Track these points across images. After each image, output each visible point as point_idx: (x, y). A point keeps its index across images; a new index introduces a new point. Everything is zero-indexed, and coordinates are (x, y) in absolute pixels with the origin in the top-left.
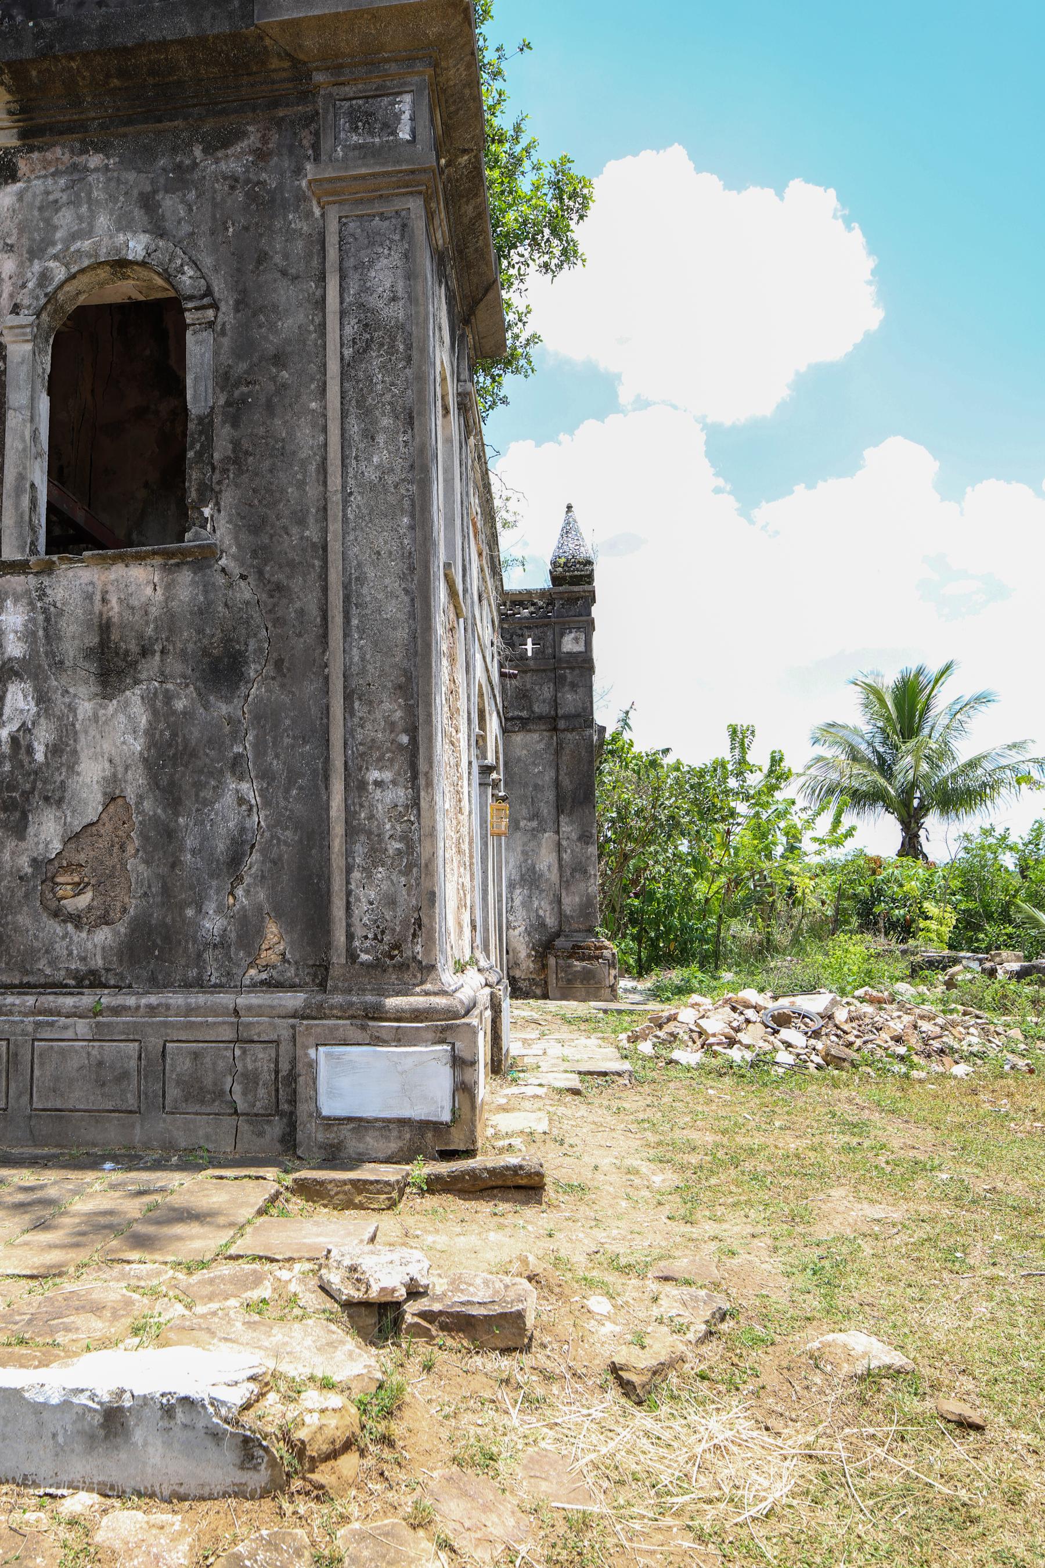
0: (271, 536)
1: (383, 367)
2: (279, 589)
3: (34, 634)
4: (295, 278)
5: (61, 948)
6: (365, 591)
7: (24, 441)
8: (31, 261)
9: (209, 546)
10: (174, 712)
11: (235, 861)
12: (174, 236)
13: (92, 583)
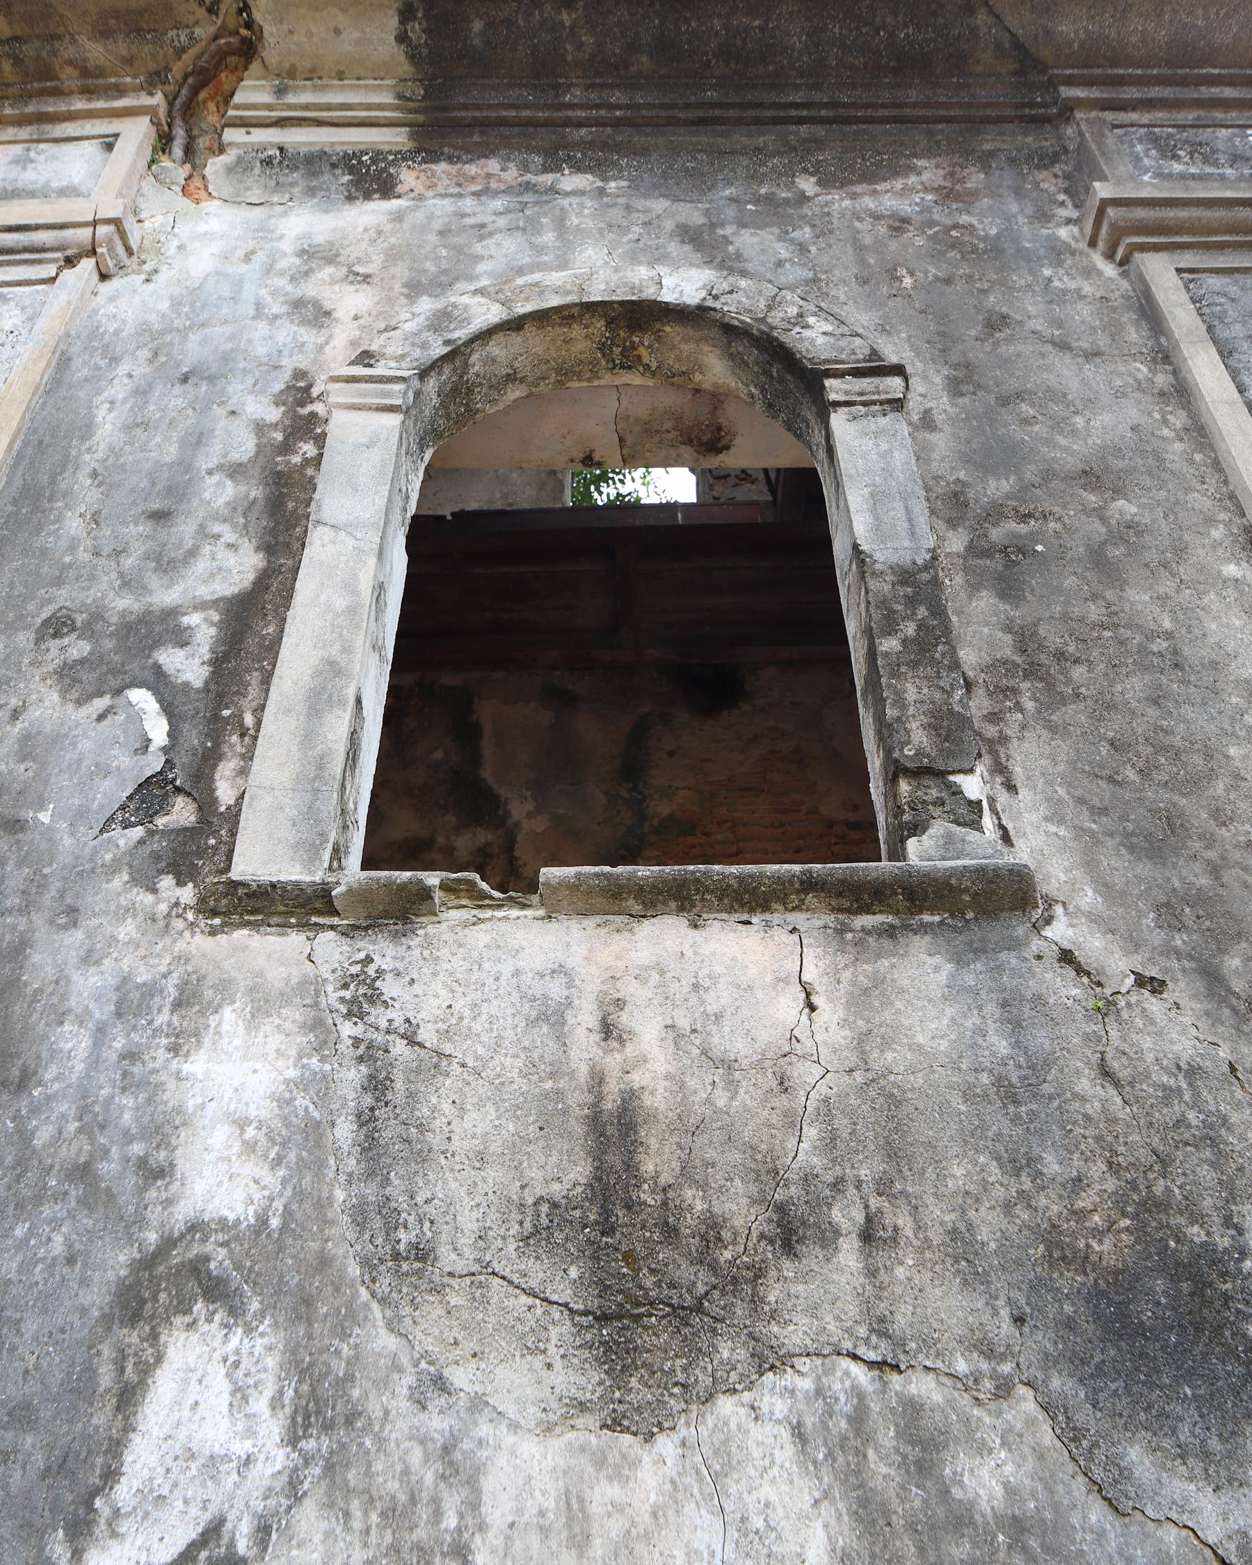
3: (314, 1133)
13: (560, 970)
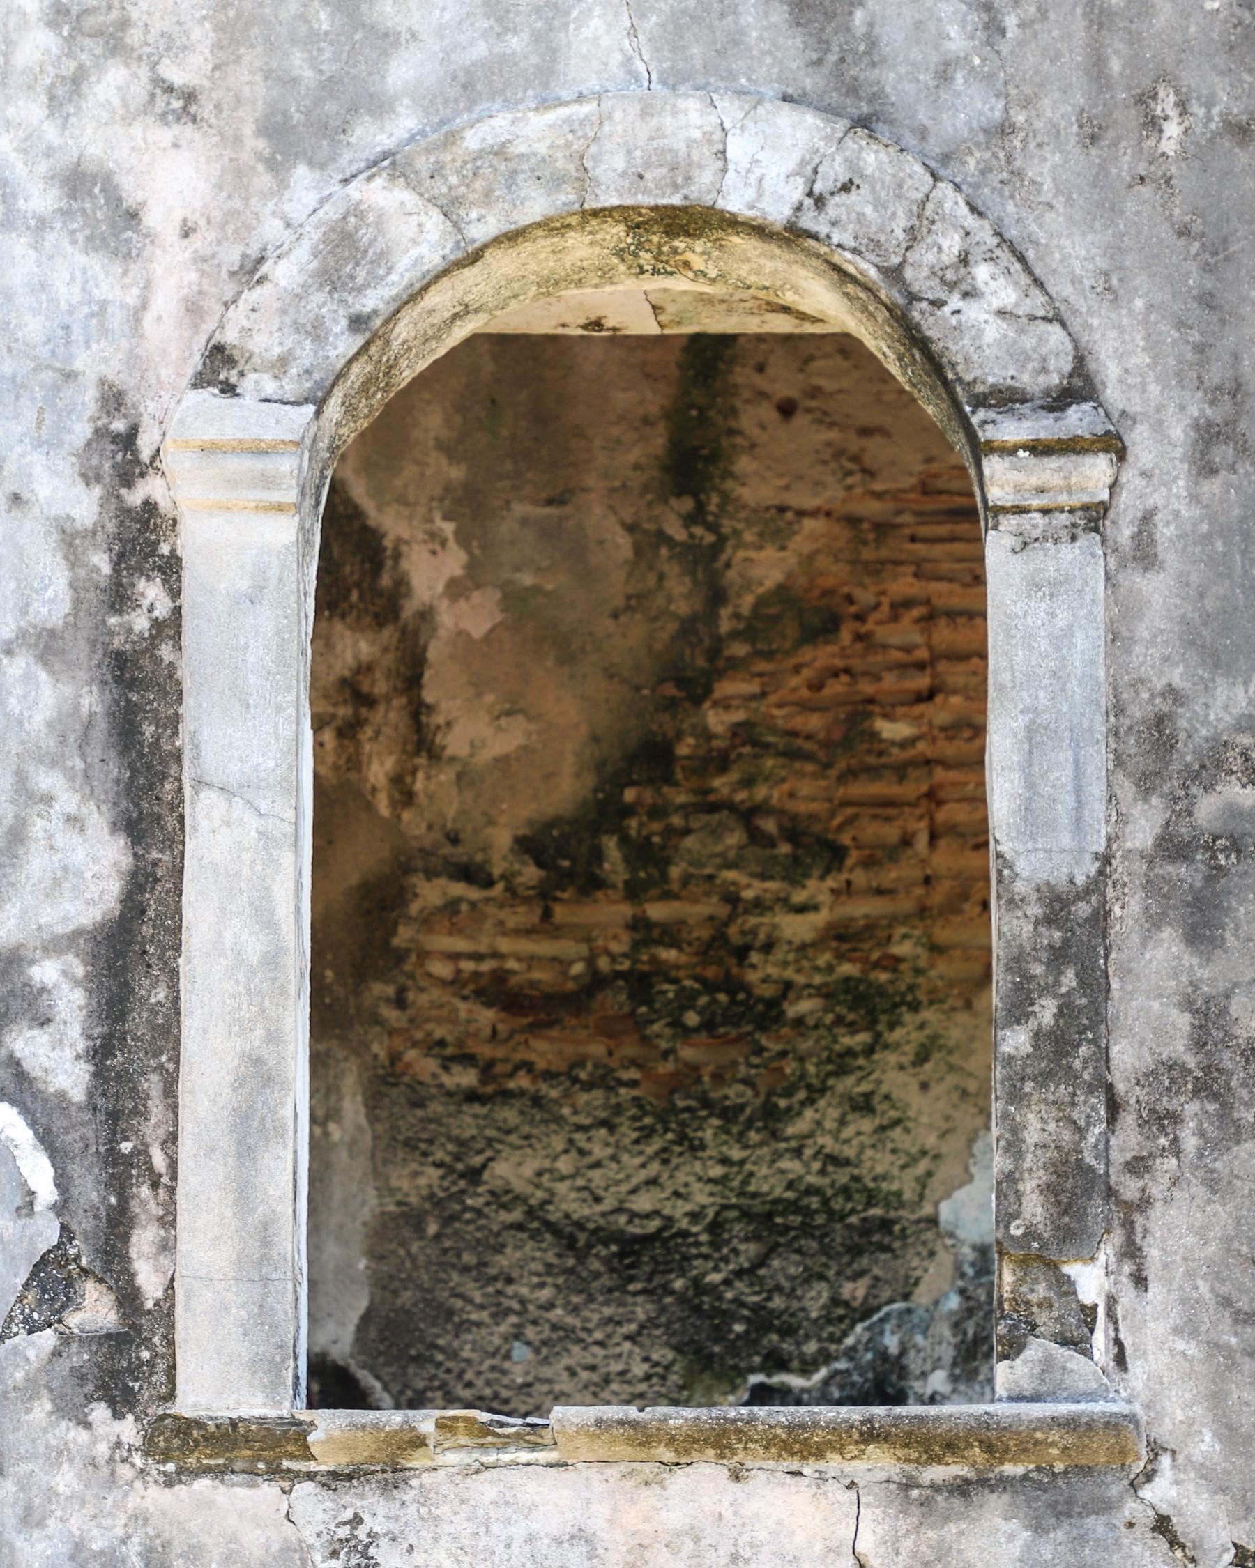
7: (269, 923)
8: (278, 165)
9: (1115, 1425)
12: (923, 133)
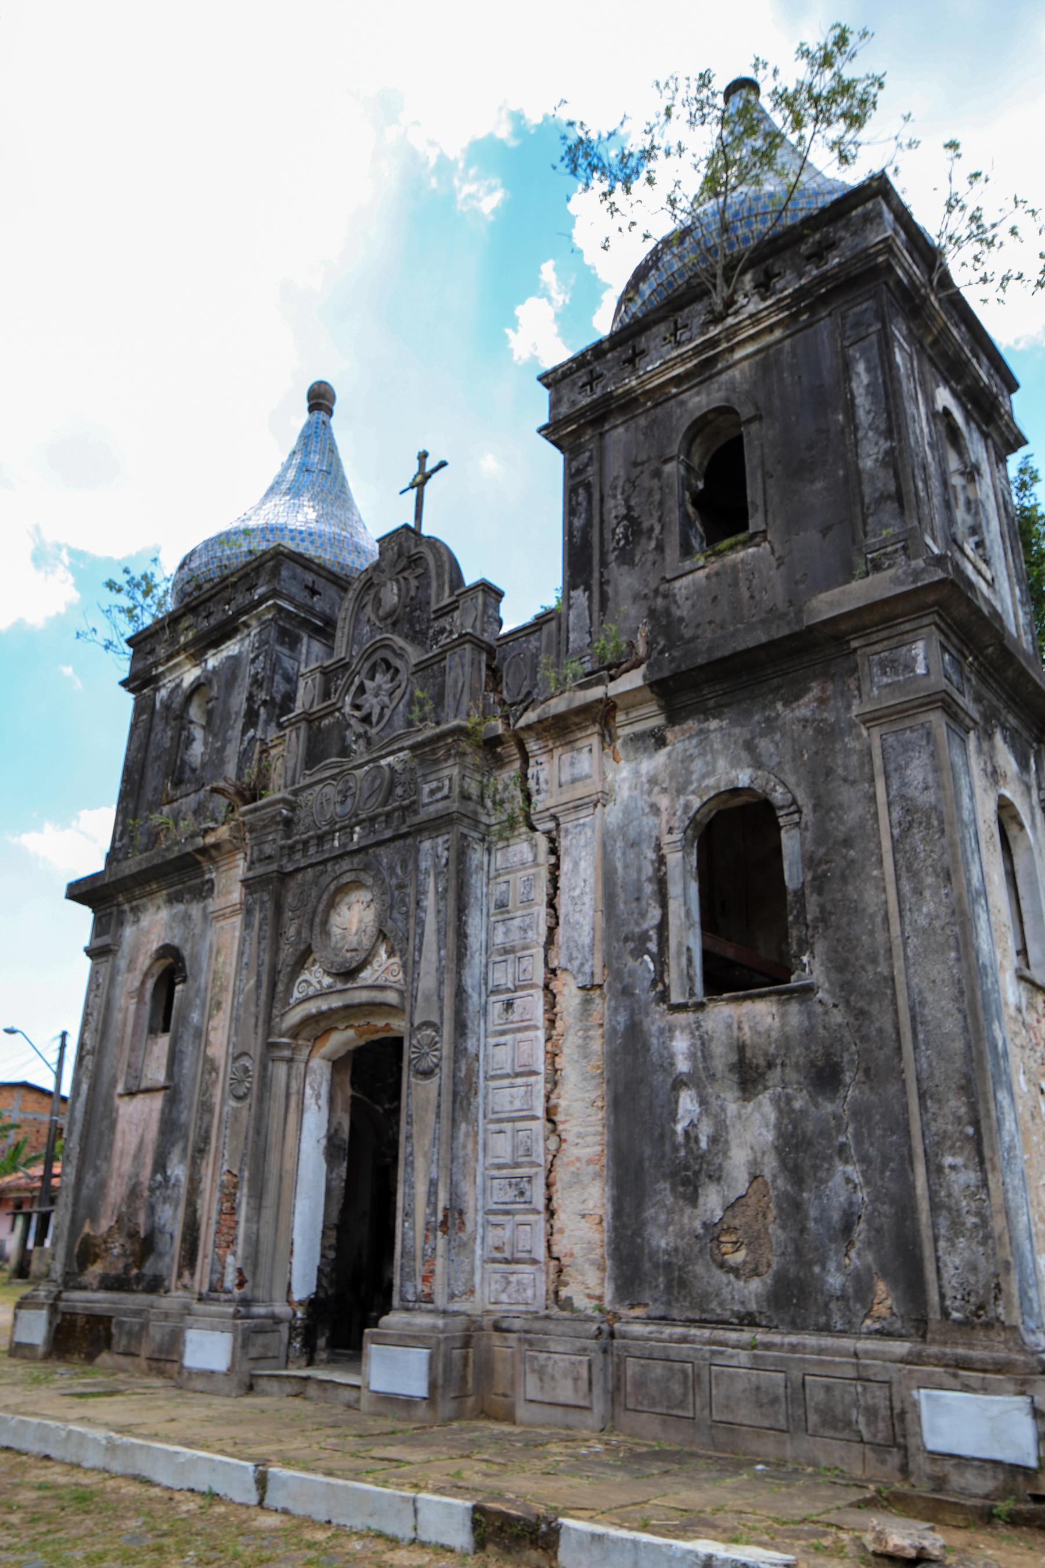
0: (853, 974)
1: (923, 839)
2: (861, 1014)
4: (854, 783)
5: (726, 1292)
6: (926, 1011)
10: (793, 1111)
11: (847, 1229)
